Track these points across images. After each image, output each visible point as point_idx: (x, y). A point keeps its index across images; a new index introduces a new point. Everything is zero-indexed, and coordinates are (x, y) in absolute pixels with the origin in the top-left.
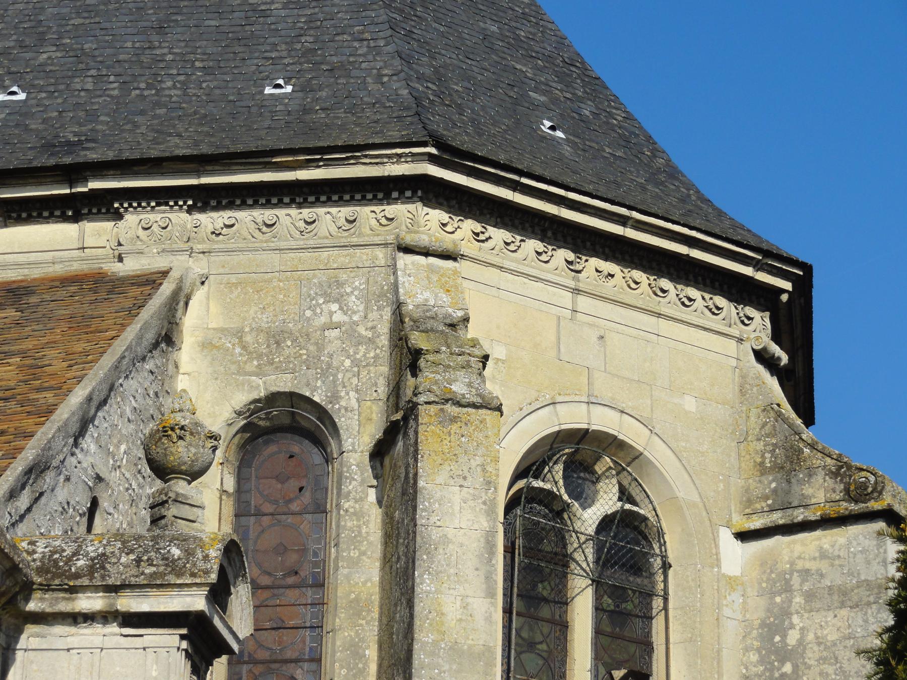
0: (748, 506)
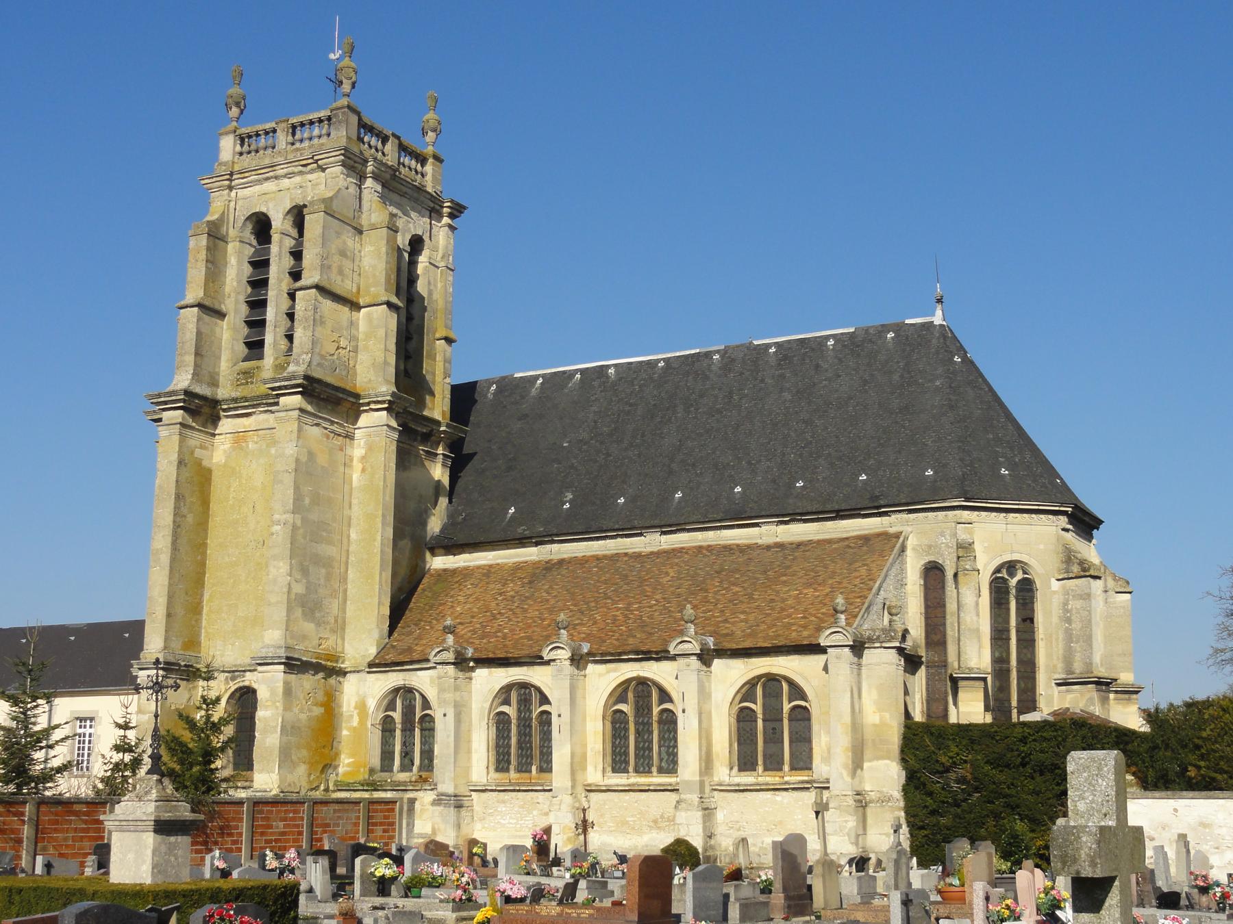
0: (1059, 571)
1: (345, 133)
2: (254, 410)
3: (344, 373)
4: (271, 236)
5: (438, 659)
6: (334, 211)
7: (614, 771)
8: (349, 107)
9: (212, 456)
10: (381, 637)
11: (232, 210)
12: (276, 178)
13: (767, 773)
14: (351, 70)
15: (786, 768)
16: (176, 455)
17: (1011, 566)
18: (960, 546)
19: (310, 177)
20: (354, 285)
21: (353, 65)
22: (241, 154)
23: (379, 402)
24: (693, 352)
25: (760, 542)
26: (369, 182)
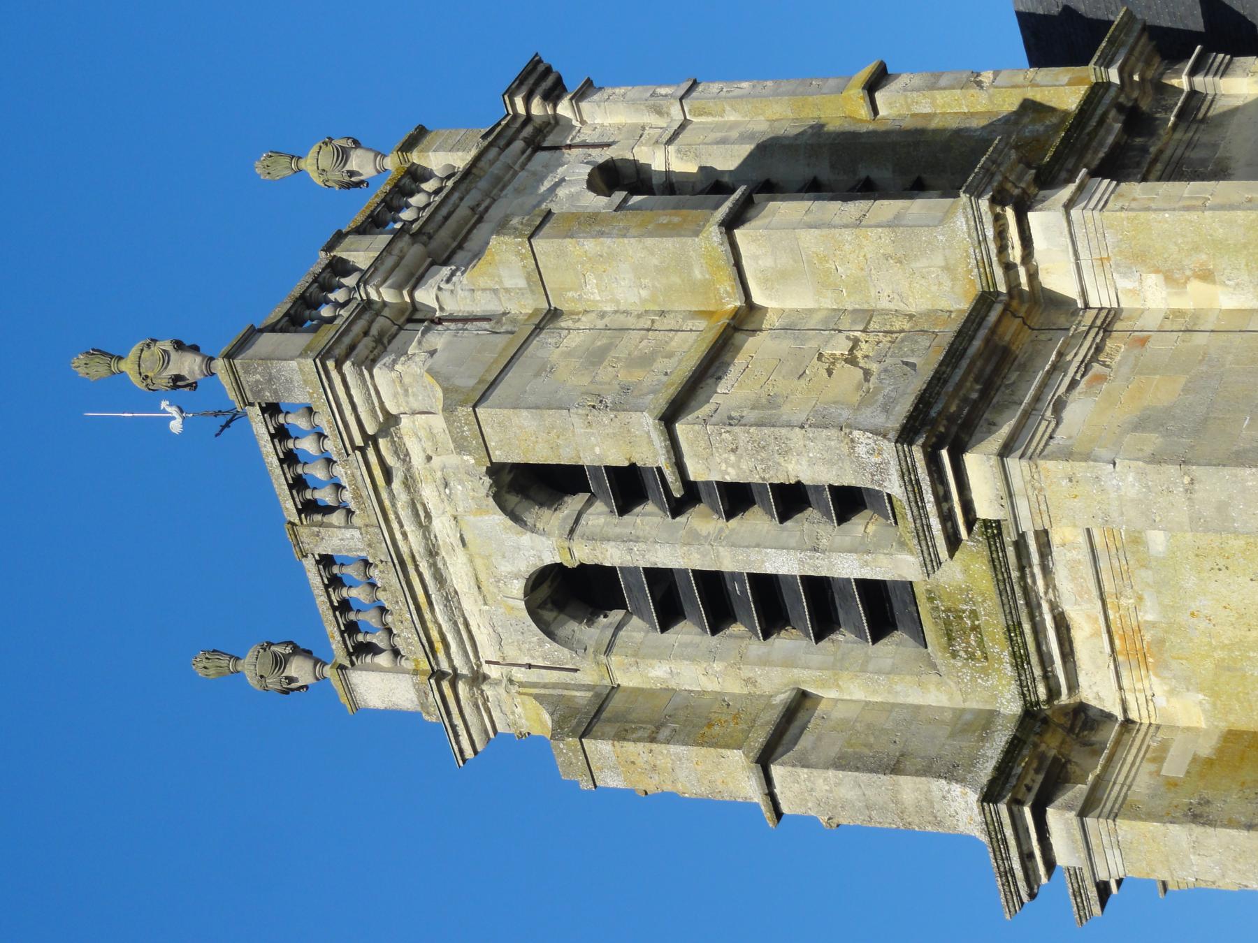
1: (294, 364)
2: (1045, 607)
3: (924, 342)
4: (582, 566)
6: (481, 382)
8: (230, 356)
9: (1188, 729)
11: (533, 676)
12: (432, 553)
14: (146, 354)
16: (1175, 829)
19: (417, 460)
20: (689, 324)
21: (135, 350)
22: (396, 653)
23: (1001, 235)
26: (425, 296)
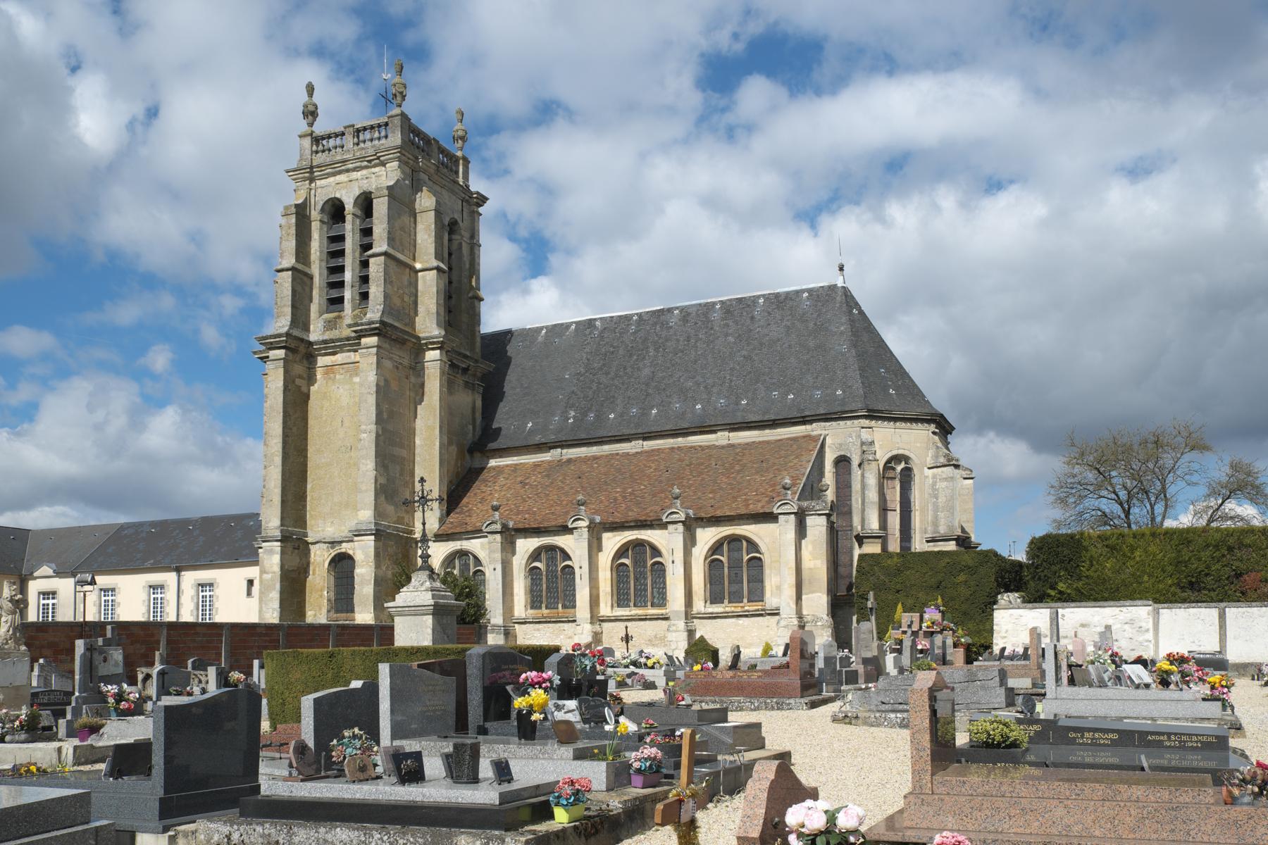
5: (488, 529)
7: (619, 606)
10: (442, 515)
11: (312, 196)
13: (731, 605)
15: (745, 600)
17: (897, 458)
18: (863, 443)
19: (374, 170)
22: (317, 152)
24: (659, 308)
25: (717, 443)
